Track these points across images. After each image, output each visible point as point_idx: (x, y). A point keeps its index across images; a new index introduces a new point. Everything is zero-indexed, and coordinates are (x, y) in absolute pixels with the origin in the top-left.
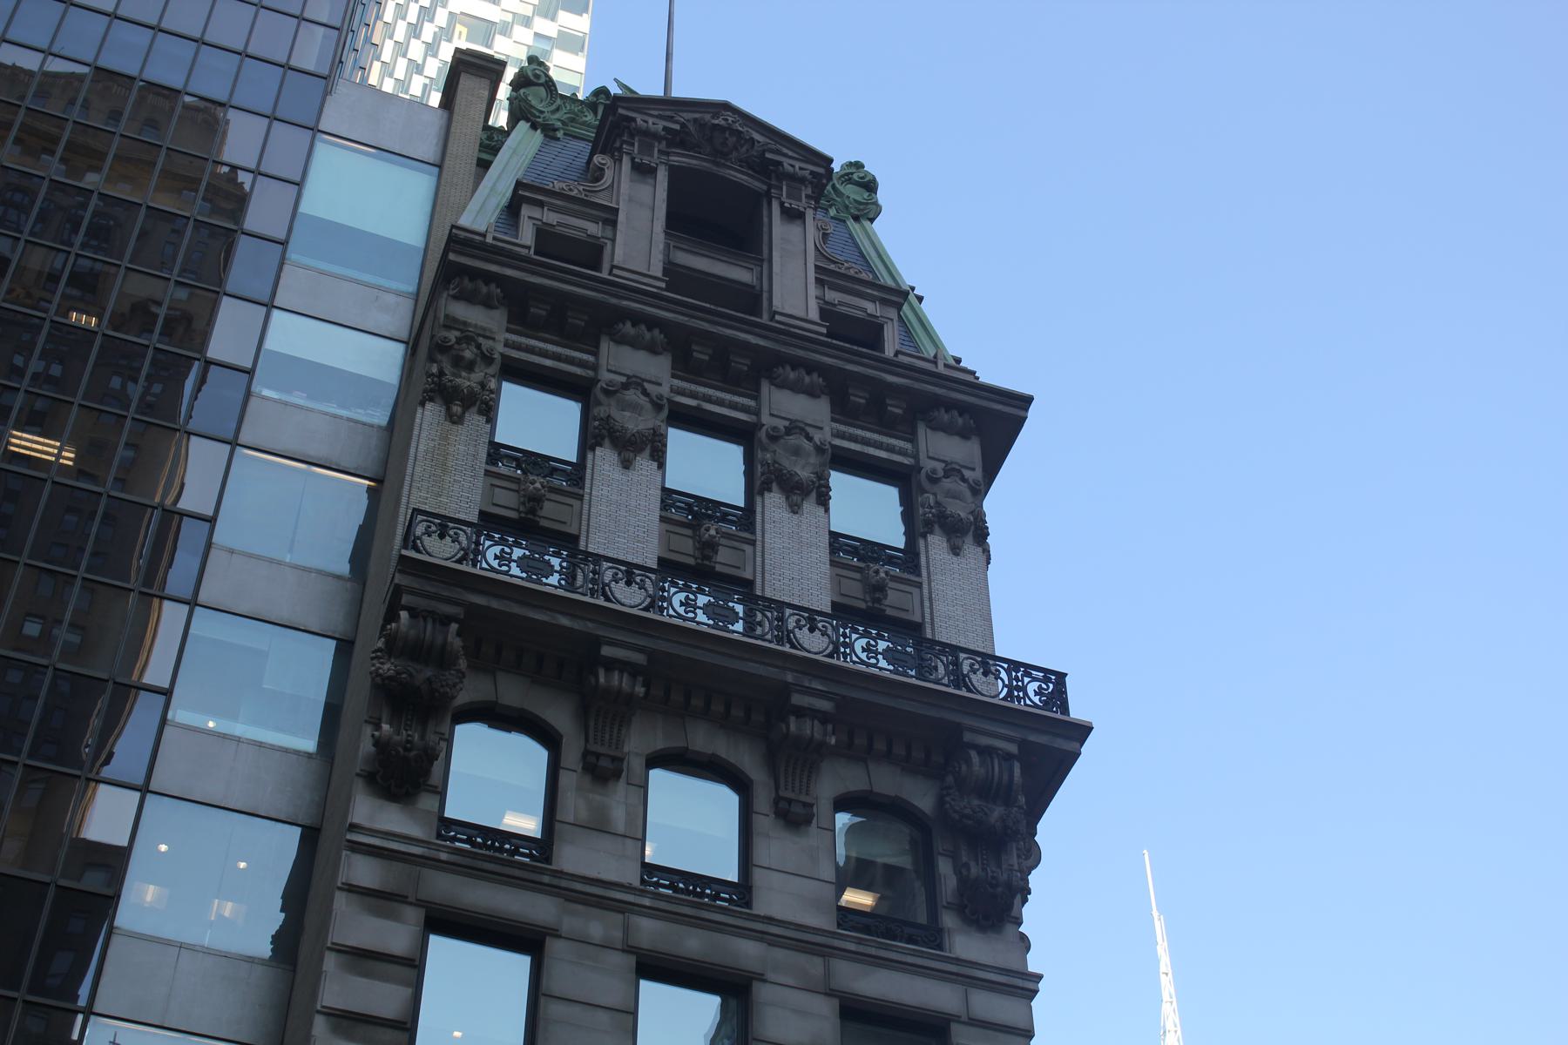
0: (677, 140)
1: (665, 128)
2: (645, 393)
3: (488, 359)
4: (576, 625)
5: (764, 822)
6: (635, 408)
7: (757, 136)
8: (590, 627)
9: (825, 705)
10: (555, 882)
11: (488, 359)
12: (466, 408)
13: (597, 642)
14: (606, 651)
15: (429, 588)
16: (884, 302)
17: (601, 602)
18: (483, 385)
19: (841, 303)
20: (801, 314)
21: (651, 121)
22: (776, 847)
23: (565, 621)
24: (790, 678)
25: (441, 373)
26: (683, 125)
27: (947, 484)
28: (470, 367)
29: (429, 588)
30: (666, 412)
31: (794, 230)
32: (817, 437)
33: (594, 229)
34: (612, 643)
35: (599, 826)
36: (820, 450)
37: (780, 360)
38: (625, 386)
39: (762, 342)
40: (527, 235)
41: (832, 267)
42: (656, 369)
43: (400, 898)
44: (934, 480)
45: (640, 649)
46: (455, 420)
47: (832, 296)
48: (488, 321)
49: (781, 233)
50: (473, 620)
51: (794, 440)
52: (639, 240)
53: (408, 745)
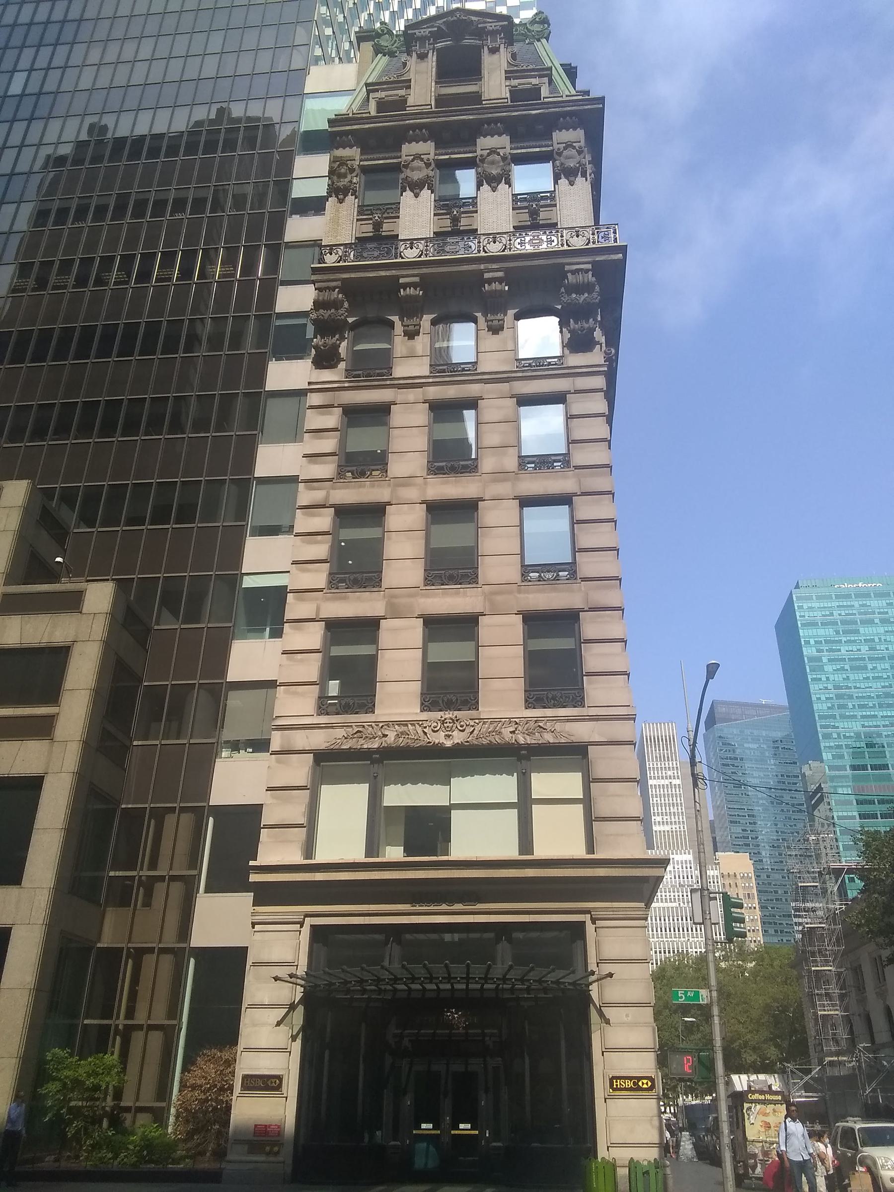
0: (438, 36)
1: (430, 32)
2: (422, 160)
3: (352, 170)
4: (388, 273)
5: (484, 333)
6: (419, 169)
7: (473, 18)
8: (394, 272)
9: (500, 274)
10: (392, 382)
11: (352, 170)
12: (345, 195)
13: (398, 277)
14: (402, 281)
15: (325, 277)
16: (541, 76)
17: (401, 260)
18: (351, 182)
19: (519, 84)
20: (500, 97)
21: (422, 31)
22: (491, 341)
23: (383, 273)
24: (482, 267)
25: (333, 183)
26: (439, 27)
27: (565, 153)
28: (345, 176)
29: (325, 277)
30: (433, 165)
31: (496, 57)
32: (502, 152)
33: (402, 92)
34: (403, 276)
35: (412, 356)
36: (504, 158)
37: (481, 122)
38: (413, 160)
39: (471, 117)
40: (372, 109)
41: (515, 68)
42: (427, 148)
43: (332, 406)
44: (560, 154)
46: (341, 201)
47: (515, 82)
48: (353, 153)
49: (487, 59)
51: (490, 158)
52: (423, 88)
53: (325, 345)
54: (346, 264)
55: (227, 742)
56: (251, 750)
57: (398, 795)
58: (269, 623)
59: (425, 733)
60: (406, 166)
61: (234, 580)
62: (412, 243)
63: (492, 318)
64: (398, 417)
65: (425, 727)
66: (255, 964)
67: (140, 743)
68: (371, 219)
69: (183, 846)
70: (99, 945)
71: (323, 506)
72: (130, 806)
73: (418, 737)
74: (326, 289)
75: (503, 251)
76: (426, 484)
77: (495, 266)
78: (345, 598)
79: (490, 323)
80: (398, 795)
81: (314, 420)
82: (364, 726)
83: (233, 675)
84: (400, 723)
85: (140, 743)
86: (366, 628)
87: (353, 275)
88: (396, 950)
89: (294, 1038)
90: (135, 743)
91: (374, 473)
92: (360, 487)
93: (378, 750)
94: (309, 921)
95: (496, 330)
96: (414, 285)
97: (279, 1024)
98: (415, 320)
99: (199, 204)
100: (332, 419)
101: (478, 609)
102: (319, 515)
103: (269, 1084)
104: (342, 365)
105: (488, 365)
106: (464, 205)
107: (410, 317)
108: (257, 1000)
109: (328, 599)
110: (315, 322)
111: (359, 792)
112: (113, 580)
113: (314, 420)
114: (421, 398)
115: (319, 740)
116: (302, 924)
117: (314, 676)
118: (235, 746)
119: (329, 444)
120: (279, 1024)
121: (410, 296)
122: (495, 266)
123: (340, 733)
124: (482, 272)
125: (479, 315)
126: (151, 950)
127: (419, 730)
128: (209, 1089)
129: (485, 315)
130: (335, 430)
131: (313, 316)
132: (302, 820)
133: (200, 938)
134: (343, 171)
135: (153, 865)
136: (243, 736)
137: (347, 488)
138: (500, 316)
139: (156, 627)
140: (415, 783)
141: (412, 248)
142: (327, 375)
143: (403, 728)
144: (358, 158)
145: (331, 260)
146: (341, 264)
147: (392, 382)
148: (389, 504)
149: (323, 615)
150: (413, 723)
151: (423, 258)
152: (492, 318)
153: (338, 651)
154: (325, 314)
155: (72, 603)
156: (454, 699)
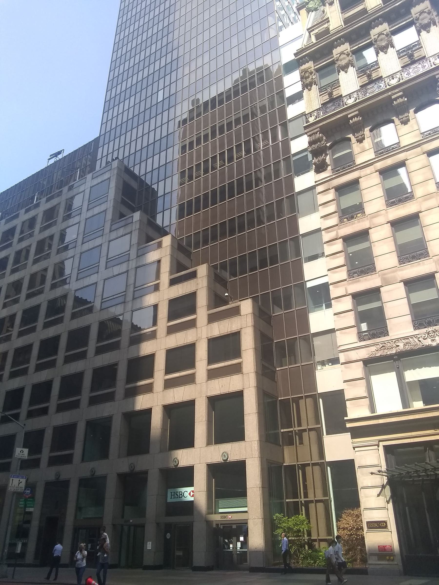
3: (311, 73)
4: (341, 115)
5: (400, 126)
6: (344, 58)
9: (401, 93)
10: (357, 167)
11: (311, 73)
12: (311, 86)
14: (349, 116)
18: (312, 79)
25: (304, 83)
28: (308, 77)
38: (340, 56)
43: (329, 189)
45: (356, 111)
46: (310, 90)
48: (310, 65)
50: (323, 130)
54: (320, 118)
55: (318, 362)
56: (331, 364)
57: (412, 375)
58: (323, 302)
59: (420, 341)
60: (337, 60)
61: (302, 285)
62: (349, 96)
63: (402, 117)
64: (363, 184)
65: (419, 338)
66: (359, 467)
67: (280, 369)
68: (326, 92)
69: (311, 414)
70: (284, 464)
71: (336, 239)
72: (282, 398)
73: (415, 344)
74: (312, 134)
75: (399, 81)
76: (387, 213)
77: (396, 91)
78: (359, 281)
79: (401, 120)
80: (412, 375)
81: (322, 199)
82: (385, 343)
83: (314, 329)
84: (405, 338)
85: (280, 369)
86: (374, 293)
87: (324, 123)
88: (432, 454)
89: (388, 502)
90: (277, 369)
91: (358, 215)
92: (353, 224)
93: (396, 354)
94: (381, 444)
95: (405, 122)
96: (356, 116)
97: (378, 495)
98: (361, 133)
99: (246, 118)
100: (331, 195)
101: (433, 270)
102: (335, 244)
103: (380, 525)
104: (329, 168)
105: (406, 141)
106: (372, 66)
107: (358, 132)
108: (365, 485)
109: (350, 284)
110: (311, 152)
111: (392, 376)
112: (250, 298)
113: (322, 199)
114: (374, 170)
115: (364, 354)
116: (378, 446)
117: (353, 323)
118: (323, 363)
119: (332, 208)
120: (378, 495)
121: (356, 122)
122: (396, 91)
123: (373, 349)
124: (390, 96)
125: (394, 118)
126: (308, 465)
127: (416, 340)
128: (351, 529)
129: (397, 117)
130: (333, 200)
131: (310, 149)
132: (365, 394)
133: (330, 457)
134: (307, 75)
135: (300, 425)
136: (325, 358)
137: (346, 227)
138: (406, 115)
139: (273, 315)
140: (420, 367)
141: (350, 98)
142: (323, 175)
143: (408, 340)
144: (312, 66)
145: (312, 120)
146: (317, 119)
147: (357, 167)
148: (370, 228)
149: (349, 292)
150: (411, 337)
151: (358, 101)
152: (402, 117)
153: (361, 308)
154: (315, 146)
155: (236, 312)
156: (431, 320)
